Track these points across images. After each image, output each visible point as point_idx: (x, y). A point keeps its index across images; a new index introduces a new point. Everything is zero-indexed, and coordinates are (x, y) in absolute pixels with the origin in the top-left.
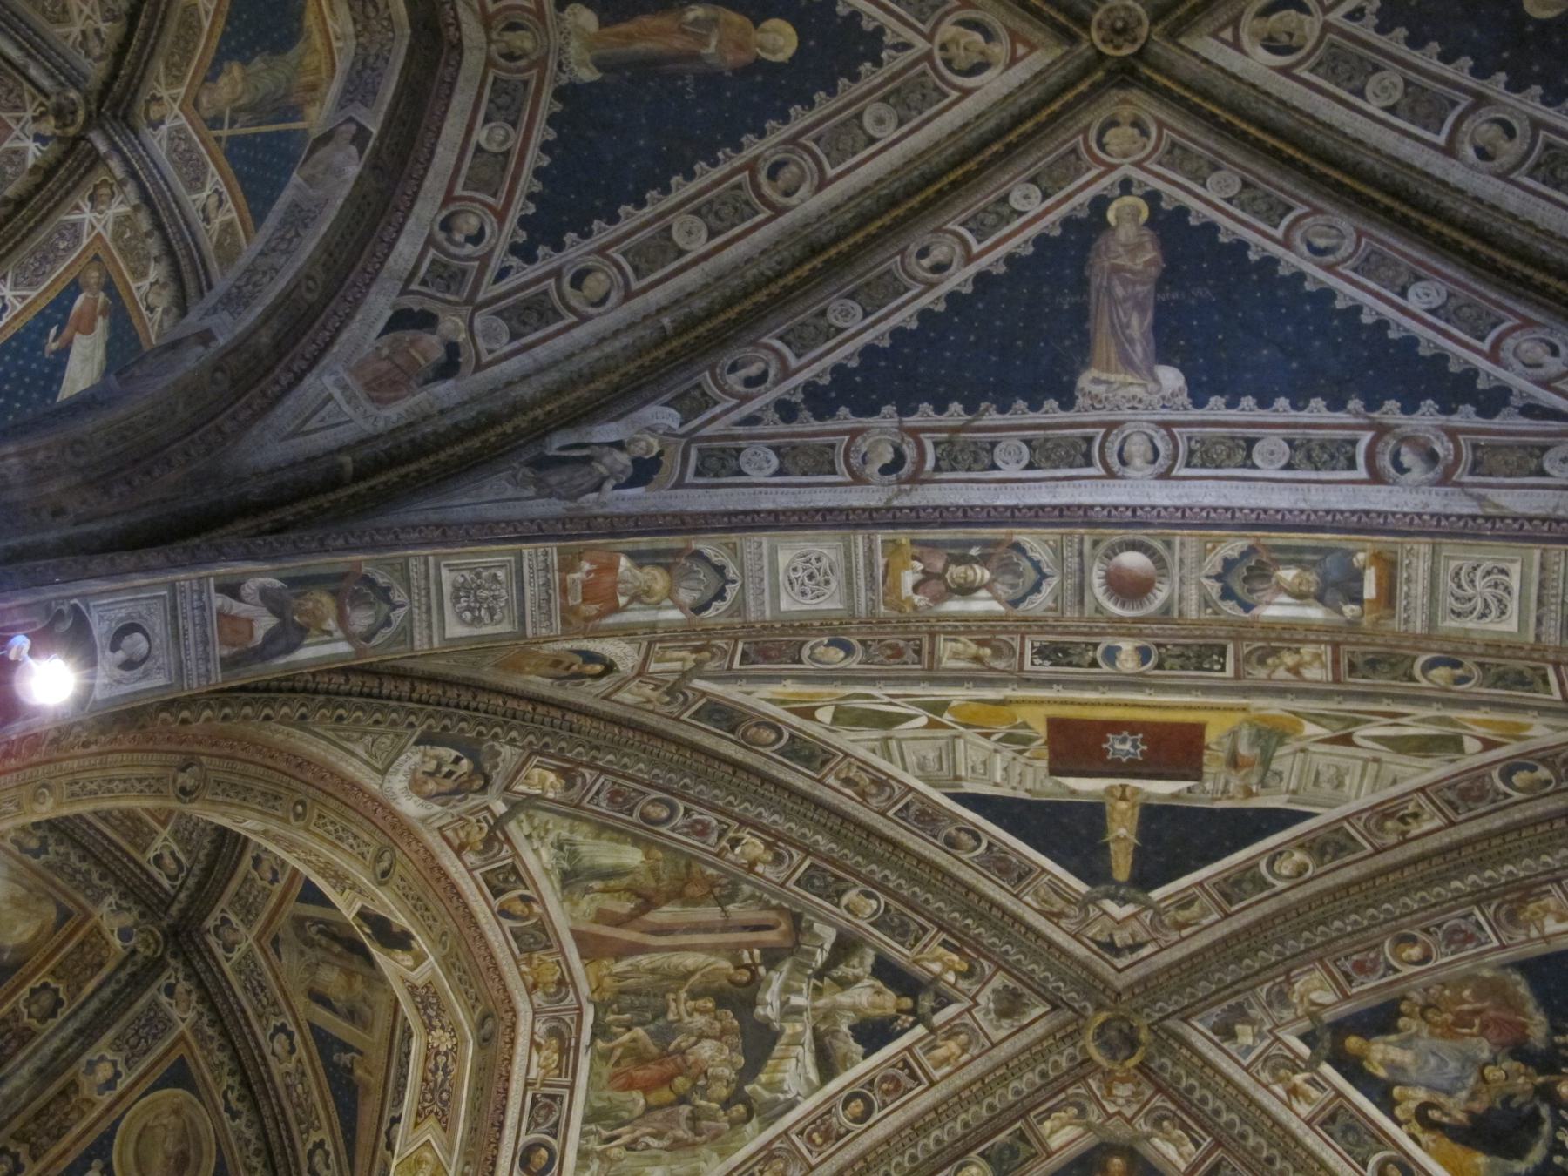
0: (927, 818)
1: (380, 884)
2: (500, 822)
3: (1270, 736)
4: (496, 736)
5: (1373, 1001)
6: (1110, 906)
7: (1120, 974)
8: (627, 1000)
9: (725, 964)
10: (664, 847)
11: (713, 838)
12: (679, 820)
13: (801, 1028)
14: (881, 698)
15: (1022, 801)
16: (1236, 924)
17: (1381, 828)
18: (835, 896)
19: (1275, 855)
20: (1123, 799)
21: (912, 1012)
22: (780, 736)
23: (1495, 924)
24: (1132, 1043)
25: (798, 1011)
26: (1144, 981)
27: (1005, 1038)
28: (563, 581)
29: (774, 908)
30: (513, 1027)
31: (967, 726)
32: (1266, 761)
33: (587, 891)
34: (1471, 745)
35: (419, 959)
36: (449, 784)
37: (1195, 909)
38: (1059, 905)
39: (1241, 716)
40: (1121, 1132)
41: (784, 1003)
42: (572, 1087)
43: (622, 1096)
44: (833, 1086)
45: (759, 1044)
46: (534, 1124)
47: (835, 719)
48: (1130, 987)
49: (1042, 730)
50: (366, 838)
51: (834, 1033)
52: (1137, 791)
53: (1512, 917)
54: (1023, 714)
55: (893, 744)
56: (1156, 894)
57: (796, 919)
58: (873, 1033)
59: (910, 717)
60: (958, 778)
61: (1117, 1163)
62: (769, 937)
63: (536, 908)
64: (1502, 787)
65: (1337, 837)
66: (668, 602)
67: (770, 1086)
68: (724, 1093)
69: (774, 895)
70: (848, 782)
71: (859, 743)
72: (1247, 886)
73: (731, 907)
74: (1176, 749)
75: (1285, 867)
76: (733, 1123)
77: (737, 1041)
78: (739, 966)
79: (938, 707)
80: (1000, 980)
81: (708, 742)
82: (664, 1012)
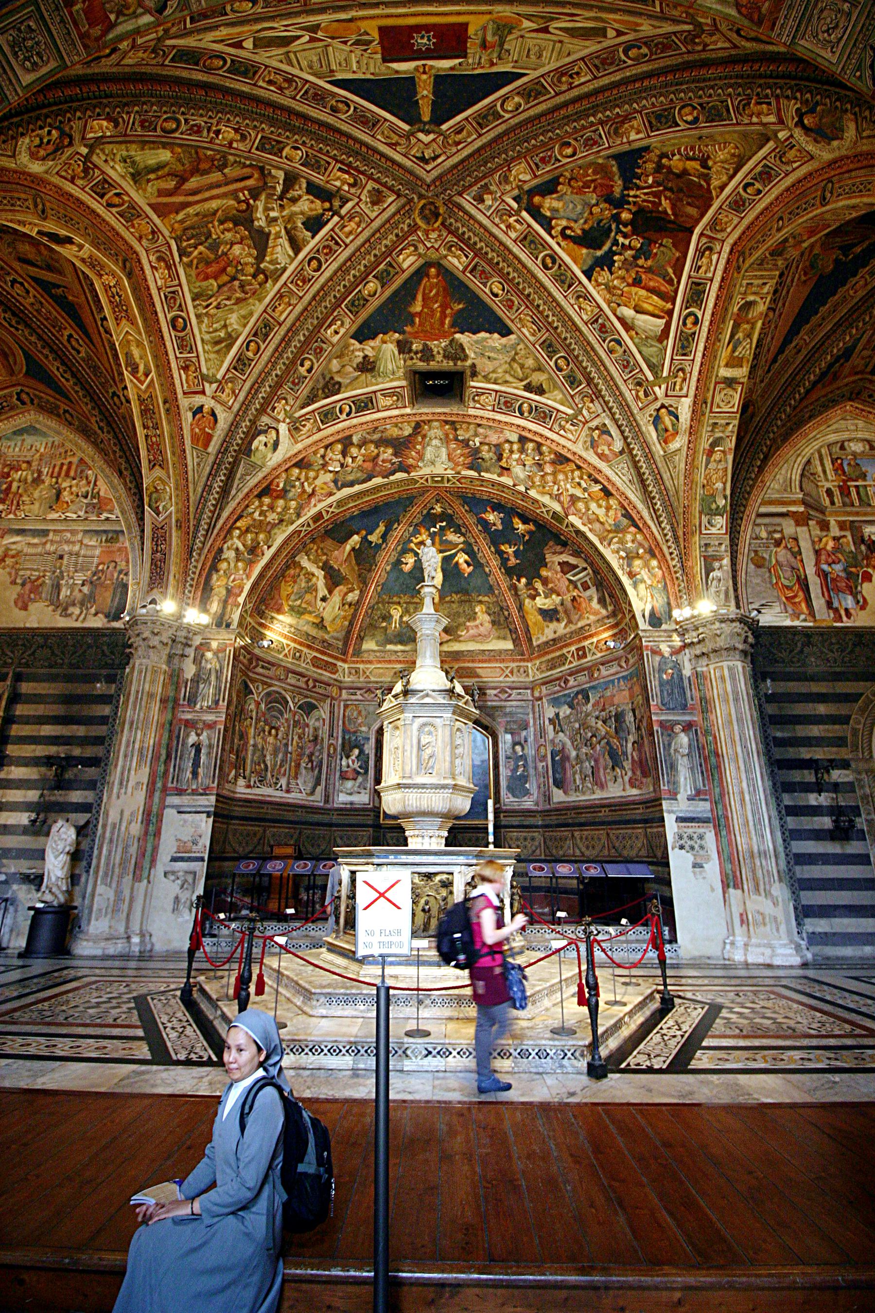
0: (319, 97)
1: (45, 219)
2: (87, 158)
3: (504, 28)
4: (69, 120)
5: (547, 177)
6: (421, 136)
7: (429, 174)
8: (190, 232)
9: (232, 202)
10: (180, 146)
11: (205, 133)
12: (183, 127)
13: (277, 229)
14: (279, 28)
15: (368, 80)
16: (484, 140)
17: (560, 81)
18: (279, 153)
19: (505, 99)
20: (423, 72)
21: (330, 209)
22: (225, 62)
23: (608, 134)
24: (437, 215)
25: (275, 220)
26: (440, 177)
27: (377, 215)
28: (71, 14)
29: (251, 166)
30: (139, 261)
31: (333, 38)
32: (501, 45)
33: (149, 181)
34: (611, 33)
35: (81, 247)
36: (51, 148)
37: (464, 133)
38: (396, 138)
39: (488, 17)
40: (433, 255)
41: (267, 217)
42: (180, 285)
43: (205, 284)
44: (301, 256)
45: (261, 241)
46: (170, 308)
47: (255, 46)
48: (434, 181)
49: (376, 35)
50: (23, 196)
51: (295, 228)
52: (432, 67)
53: (616, 132)
54: (364, 25)
55: (292, 56)
56: (444, 127)
57: (262, 169)
58: (314, 224)
59: (299, 37)
60: (332, 71)
61: (433, 271)
62: (250, 182)
63: (126, 198)
64: (623, 58)
65: (538, 87)
66: (140, 10)
67: (271, 262)
68: (252, 271)
69: (246, 158)
70: (270, 82)
71: (271, 58)
72: (490, 118)
73: (226, 171)
74: (452, 40)
75: (509, 106)
76: (260, 284)
77: (250, 242)
78: (239, 202)
79: (314, 29)
80: (371, 185)
81: (185, 74)
82: (209, 235)
